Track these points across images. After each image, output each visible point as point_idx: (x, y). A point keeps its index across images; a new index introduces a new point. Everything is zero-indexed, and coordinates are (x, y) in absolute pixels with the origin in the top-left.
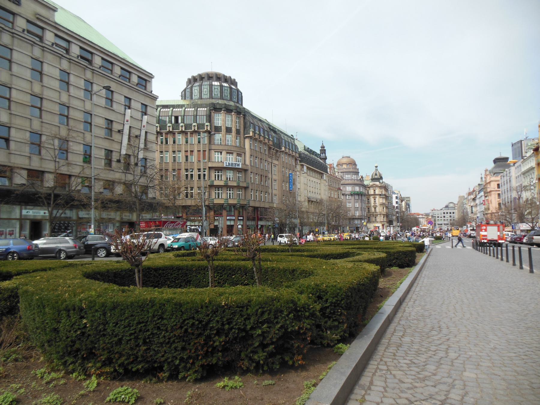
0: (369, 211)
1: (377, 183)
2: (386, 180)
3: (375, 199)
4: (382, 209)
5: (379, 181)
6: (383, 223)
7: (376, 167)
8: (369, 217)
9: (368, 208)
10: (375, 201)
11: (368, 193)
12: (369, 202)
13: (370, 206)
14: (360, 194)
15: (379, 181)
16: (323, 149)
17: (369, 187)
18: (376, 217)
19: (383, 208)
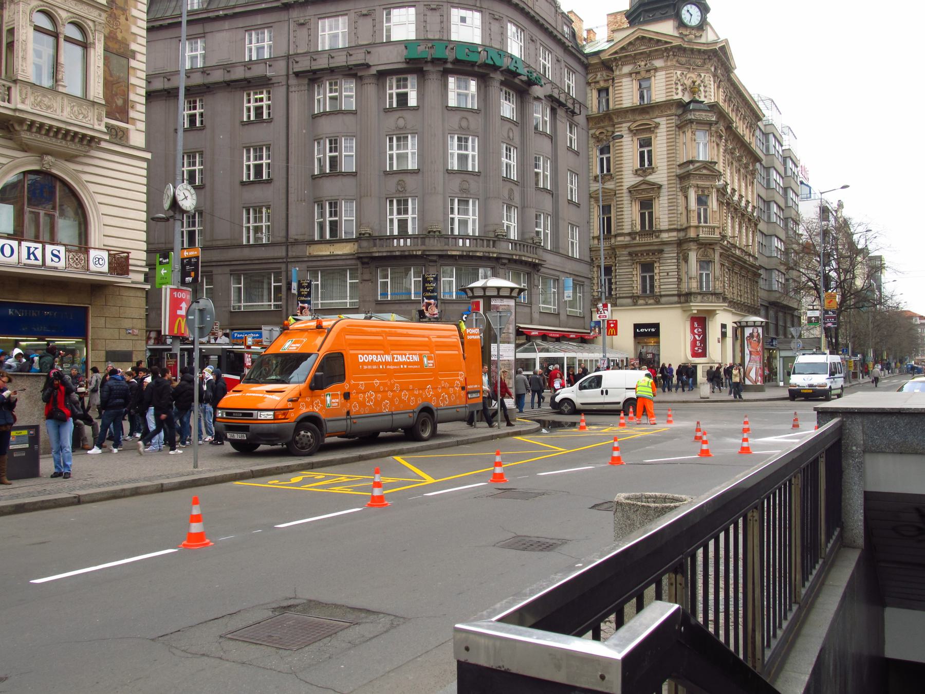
5: (678, 17)
6: (697, 306)
9: (606, 209)
10: (646, 165)
12: (608, 173)
13: (615, 193)
18: (648, 268)
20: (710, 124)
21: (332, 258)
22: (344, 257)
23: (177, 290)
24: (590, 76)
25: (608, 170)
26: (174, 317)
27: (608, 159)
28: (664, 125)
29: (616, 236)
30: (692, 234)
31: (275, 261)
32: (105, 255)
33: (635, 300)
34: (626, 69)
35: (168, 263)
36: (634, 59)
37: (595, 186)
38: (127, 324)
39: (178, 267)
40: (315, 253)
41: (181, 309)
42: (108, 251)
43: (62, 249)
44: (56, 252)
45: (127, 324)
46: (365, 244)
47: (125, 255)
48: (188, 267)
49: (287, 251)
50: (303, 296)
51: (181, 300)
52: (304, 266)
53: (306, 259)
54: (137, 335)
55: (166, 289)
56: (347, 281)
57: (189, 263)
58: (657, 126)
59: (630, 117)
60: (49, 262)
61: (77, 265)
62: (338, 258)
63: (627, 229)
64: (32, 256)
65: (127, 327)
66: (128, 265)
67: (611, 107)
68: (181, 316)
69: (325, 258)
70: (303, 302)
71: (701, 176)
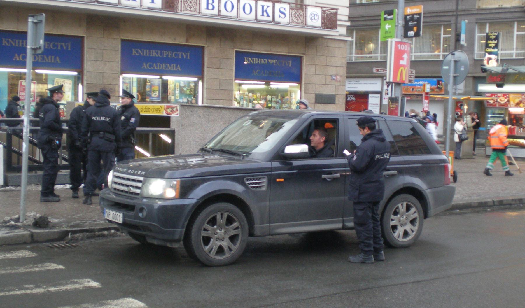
21: (501, 11)
22: (512, 10)
23: (401, 43)
26: (397, 66)
31: (446, 14)
32: (319, 11)
35: (392, 19)
38: (332, 71)
39: (401, 22)
40: (484, 6)
41: (403, 59)
42: (322, 8)
43: (287, 7)
44: (282, 10)
45: (332, 71)
47: (334, 11)
48: (411, 23)
49: (457, 5)
50: (490, 47)
51: (403, 52)
52: (473, 18)
53: (475, 12)
54: (339, 81)
55: (392, 42)
56: (513, 32)
57: (412, 19)
60: (277, 19)
61: (298, 20)
62: (507, 10)
64: (265, 14)
65: (332, 74)
66: (336, 20)
68: (404, 66)
69: (494, 11)
70: (490, 53)
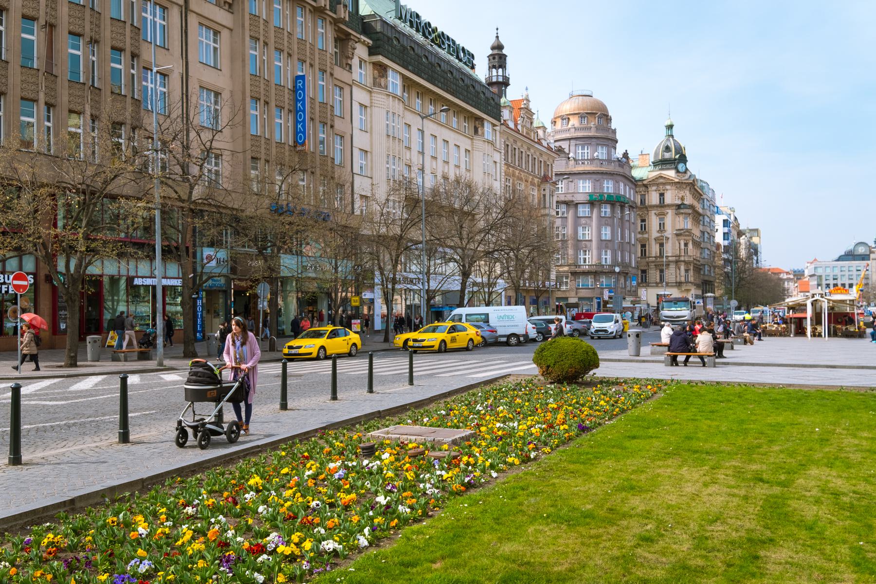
0: (644, 253)
1: (671, 174)
2: (695, 167)
3: (661, 219)
4: (683, 247)
7: (670, 127)
8: (644, 272)
9: (643, 246)
11: (643, 202)
12: (644, 229)
14: (616, 202)
15: (676, 169)
16: (496, 52)
17: (646, 186)
18: (662, 271)
19: (686, 245)
20: (690, 214)
24: (637, 189)
25: (645, 229)
27: (645, 225)
28: (670, 213)
29: (649, 257)
30: (682, 259)
33: (656, 285)
34: (654, 188)
36: (658, 185)
37: (639, 236)
46: (572, 267)
58: (667, 213)
59: (655, 208)
63: (654, 255)
67: (647, 202)
71: (686, 235)
